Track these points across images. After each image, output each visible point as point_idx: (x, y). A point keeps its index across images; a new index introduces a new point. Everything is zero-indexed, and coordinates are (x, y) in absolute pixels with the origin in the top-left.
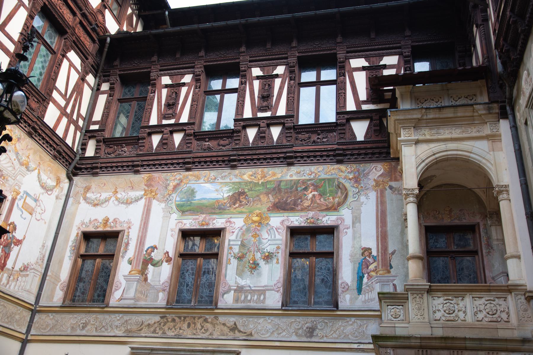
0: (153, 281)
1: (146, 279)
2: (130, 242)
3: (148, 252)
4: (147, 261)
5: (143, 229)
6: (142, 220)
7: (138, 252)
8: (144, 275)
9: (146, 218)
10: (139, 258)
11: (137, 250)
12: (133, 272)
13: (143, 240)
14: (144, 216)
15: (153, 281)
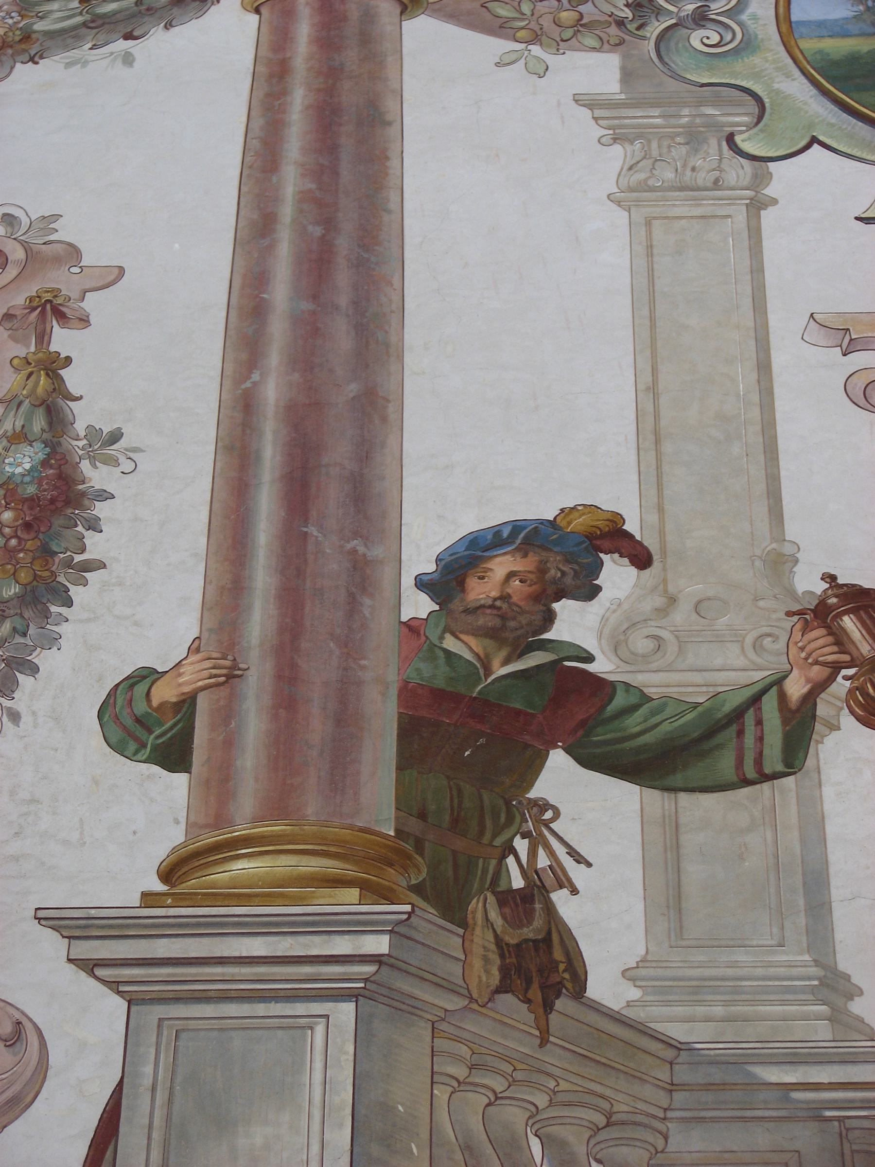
0: (697, 990)
1: (542, 967)
2: (96, 476)
3: (480, 590)
4: (483, 708)
5: (310, 331)
6: (257, 228)
7: (292, 598)
8: (484, 909)
9: (321, 205)
10: (319, 671)
11: (263, 577)
12: (243, 867)
13: (338, 453)
14: (291, 181)
15: (697, 990)
